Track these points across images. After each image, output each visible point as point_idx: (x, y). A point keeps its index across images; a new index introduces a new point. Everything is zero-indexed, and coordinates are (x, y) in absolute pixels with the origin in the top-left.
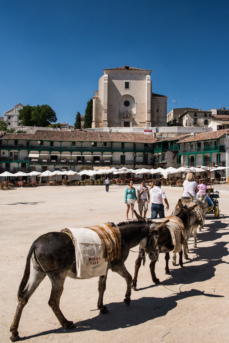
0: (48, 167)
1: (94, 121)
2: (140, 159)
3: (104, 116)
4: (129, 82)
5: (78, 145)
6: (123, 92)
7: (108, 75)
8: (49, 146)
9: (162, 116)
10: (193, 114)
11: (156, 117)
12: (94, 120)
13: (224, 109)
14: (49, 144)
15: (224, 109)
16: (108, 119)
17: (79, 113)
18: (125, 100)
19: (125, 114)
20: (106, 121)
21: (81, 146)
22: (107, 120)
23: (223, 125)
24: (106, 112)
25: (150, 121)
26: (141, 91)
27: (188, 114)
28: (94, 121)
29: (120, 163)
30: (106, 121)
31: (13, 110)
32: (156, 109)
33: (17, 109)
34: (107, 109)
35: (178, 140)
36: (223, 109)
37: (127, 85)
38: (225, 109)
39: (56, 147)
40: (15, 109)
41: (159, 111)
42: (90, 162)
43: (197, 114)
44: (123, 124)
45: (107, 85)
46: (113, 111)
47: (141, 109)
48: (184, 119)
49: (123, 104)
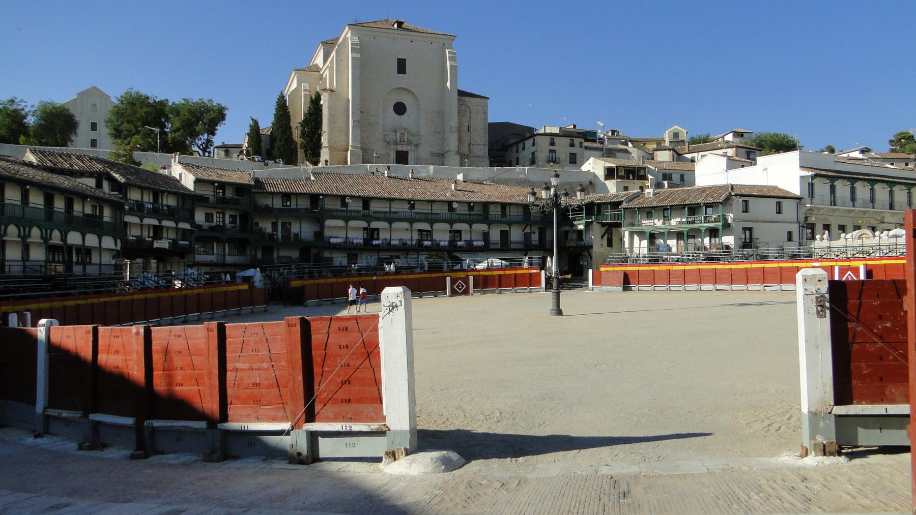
2: (535, 238)
5: (419, 208)
8: (361, 209)
11: (466, 144)
13: (575, 126)
14: (361, 204)
19: (398, 134)
21: (429, 211)
29: (499, 246)
35: (621, 203)
36: (572, 127)
37: (402, 67)
39: (375, 212)
41: (472, 130)
42: (446, 243)
43: (557, 139)
44: (393, 156)
46: (370, 124)
48: (524, 149)
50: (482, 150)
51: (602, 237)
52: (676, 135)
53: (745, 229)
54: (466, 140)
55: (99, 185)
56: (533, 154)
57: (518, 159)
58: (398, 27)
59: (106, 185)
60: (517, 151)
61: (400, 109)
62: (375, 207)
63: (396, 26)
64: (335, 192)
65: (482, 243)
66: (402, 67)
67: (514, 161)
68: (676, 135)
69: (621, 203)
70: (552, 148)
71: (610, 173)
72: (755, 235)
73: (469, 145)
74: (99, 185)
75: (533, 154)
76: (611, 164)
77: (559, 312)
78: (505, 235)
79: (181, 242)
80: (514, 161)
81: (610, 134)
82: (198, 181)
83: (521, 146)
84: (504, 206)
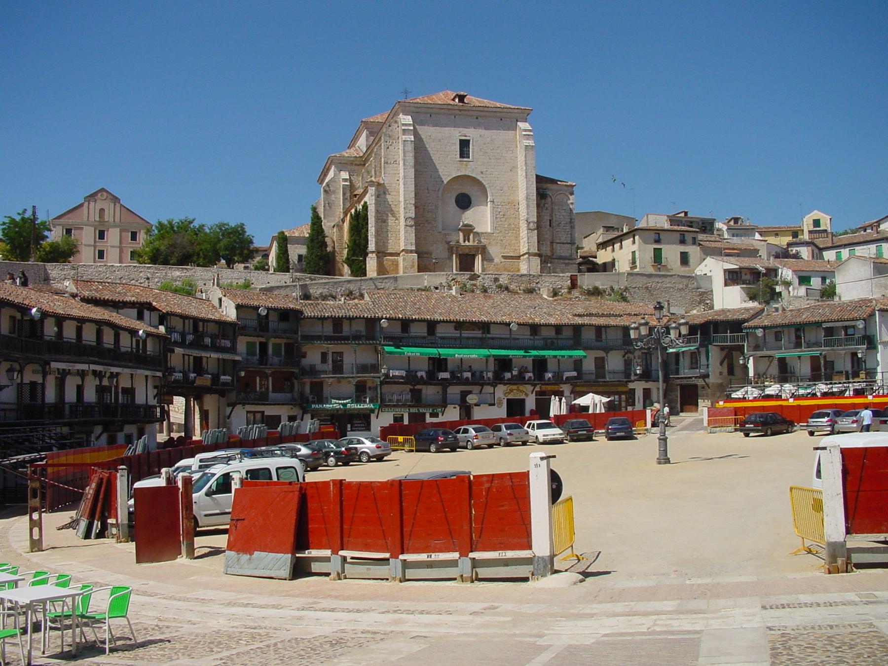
0: (424, 391)
1: (373, 252)
3: (402, 237)
4: (469, 141)
5: (495, 332)
6: (448, 167)
7: (410, 117)
9: (563, 239)
10: (653, 236)
12: (372, 246)
13: (686, 213)
15: (686, 213)
16: (417, 245)
18: (459, 192)
20: (411, 252)
22: (413, 248)
23: (740, 268)
24: (411, 226)
25: (535, 255)
26: (509, 167)
27: (637, 238)
28: (373, 252)
30: (411, 252)
31: (81, 205)
32: (548, 218)
33: (92, 204)
34: (413, 216)
36: (683, 215)
38: (689, 215)
39: (441, 338)
40: (86, 204)
45: (410, 147)
47: (503, 221)
48: (621, 248)
49: (454, 201)
51: (721, 364)
52: (817, 223)
54: (548, 236)
56: (634, 253)
58: (460, 101)
59: (147, 313)
60: (613, 250)
62: (441, 331)
63: (457, 100)
65: (575, 374)
68: (817, 223)
71: (732, 278)
73: (552, 243)
75: (634, 253)
76: (732, 264)
77: (664, 459)
78: (600, 363)
79: (222, 377)
81: (732, 223)
82: (238, 307)
84: (599, 329)
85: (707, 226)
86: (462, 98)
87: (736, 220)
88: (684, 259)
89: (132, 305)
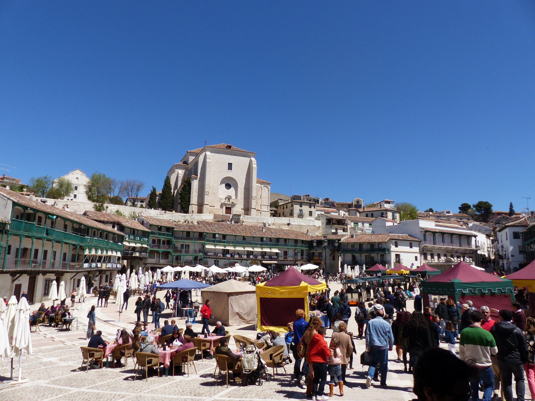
17: (154, 189)
37: (230, 166)
50: (266, 209)
53: (396, 255)
55: (113, 227)
57: (283, 213)
60: (283, 209)
61: (228, 186)
64: (211, 232)
66: (230, 166)
67: (282, 214)
68: (358, 202)
69: (340, 240)
70: (301, 208)
72: (401, 258)
74: (113, 227)
80: (282, 214)
83: (285, 206)
85: (317, 201)
86: (230, 147)
87: (327, 199)
88: (311, 214)
89: (111, 223)
